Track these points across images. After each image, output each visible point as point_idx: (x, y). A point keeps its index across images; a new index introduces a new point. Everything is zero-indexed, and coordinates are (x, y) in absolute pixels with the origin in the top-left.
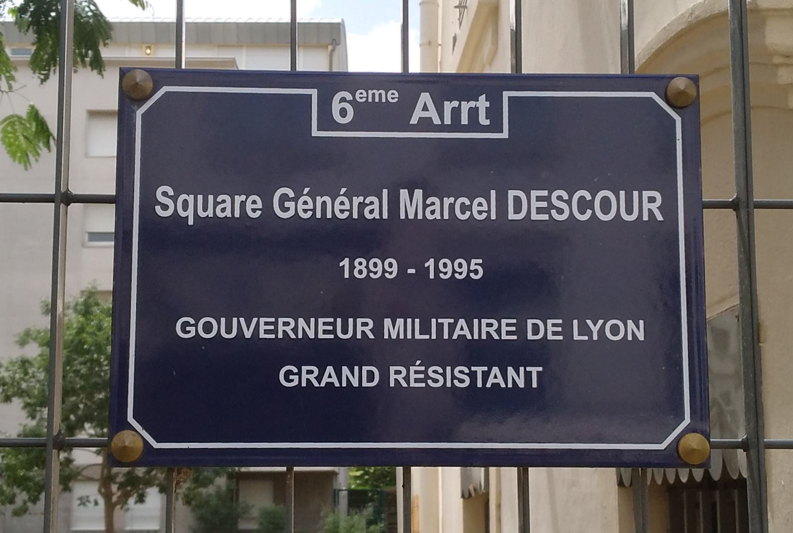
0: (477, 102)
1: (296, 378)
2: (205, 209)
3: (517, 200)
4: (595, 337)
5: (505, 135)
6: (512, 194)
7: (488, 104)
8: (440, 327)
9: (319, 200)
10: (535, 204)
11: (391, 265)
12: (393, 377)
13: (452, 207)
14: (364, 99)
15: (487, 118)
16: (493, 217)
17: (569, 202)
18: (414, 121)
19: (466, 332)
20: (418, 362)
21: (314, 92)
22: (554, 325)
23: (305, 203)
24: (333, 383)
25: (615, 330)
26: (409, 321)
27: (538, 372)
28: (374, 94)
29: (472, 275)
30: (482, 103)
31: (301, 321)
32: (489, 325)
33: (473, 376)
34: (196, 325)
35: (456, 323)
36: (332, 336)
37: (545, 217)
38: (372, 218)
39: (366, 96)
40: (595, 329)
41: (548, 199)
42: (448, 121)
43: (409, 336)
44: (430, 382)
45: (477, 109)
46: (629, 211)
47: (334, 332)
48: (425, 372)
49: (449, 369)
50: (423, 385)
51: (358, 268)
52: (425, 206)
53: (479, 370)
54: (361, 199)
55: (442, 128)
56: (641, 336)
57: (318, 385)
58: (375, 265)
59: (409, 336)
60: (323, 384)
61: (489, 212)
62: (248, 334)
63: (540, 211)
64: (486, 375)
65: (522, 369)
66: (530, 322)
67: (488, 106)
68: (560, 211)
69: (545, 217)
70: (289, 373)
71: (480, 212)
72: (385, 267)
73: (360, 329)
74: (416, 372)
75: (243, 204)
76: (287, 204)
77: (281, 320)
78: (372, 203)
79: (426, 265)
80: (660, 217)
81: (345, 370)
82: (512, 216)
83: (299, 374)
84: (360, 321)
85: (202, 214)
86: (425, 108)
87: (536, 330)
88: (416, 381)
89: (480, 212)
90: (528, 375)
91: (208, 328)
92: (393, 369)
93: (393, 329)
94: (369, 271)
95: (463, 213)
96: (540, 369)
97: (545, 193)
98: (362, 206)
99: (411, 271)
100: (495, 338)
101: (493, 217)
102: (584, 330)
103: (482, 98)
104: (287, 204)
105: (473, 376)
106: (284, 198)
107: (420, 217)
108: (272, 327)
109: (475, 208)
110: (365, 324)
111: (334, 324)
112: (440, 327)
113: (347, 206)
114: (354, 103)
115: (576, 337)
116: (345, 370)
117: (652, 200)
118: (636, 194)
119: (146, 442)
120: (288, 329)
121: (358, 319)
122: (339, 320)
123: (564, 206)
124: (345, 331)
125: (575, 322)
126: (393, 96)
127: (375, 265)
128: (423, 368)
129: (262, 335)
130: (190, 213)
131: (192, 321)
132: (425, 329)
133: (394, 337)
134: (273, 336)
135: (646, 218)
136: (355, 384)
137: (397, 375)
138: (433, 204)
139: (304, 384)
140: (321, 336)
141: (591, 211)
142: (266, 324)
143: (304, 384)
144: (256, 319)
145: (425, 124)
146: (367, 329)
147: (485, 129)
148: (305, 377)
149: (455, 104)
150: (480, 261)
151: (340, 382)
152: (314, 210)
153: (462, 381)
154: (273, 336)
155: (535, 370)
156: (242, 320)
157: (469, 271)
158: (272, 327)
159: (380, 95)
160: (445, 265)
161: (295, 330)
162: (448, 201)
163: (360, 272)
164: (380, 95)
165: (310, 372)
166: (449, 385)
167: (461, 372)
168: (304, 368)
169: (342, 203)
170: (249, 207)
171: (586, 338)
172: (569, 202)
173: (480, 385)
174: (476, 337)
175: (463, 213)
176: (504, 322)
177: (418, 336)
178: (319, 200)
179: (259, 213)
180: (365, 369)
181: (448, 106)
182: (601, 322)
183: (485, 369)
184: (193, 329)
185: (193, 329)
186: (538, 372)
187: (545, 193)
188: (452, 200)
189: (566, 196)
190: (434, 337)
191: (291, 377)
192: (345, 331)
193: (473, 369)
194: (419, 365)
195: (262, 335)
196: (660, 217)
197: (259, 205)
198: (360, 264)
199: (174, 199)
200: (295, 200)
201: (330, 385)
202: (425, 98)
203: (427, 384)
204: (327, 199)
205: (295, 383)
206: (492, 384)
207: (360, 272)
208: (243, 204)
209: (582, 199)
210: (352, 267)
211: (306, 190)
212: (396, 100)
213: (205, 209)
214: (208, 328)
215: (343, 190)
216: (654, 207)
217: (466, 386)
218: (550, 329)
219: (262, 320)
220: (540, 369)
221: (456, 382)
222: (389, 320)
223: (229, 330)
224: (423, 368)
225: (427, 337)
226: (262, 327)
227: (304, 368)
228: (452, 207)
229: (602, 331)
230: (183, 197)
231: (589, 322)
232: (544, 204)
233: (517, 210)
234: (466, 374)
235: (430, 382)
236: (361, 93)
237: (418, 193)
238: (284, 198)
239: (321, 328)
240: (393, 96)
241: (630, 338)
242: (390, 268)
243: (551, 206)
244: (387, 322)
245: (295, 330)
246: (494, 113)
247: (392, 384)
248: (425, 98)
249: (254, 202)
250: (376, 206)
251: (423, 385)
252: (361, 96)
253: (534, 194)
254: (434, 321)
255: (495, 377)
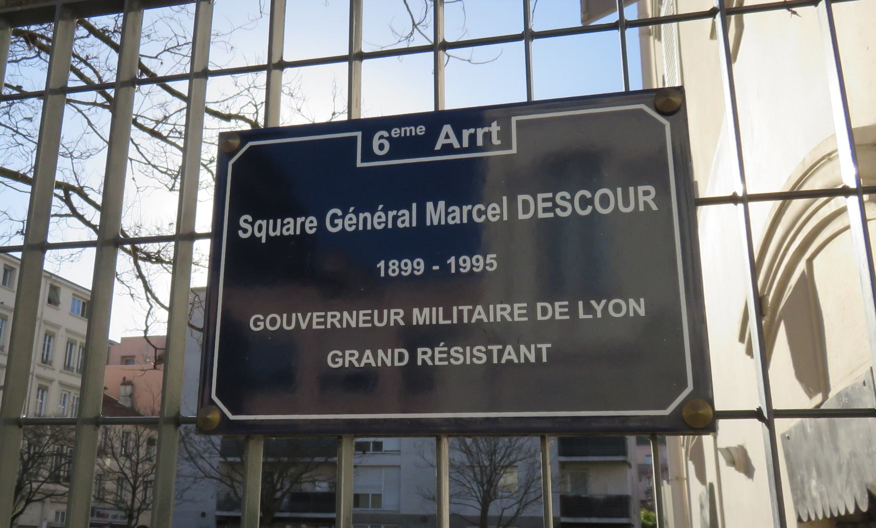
0: (490, 128)
1: (340, 360)
2: (274, 230)
3: (526, 203)
4: (599, 315)
5: (514, 151)
6: (521, 198)
7: (499, 128)
8: (460, 313)
9: (362, 216)
10: (541, 205)
11: (418, 264)
12: (420, 357)
13: (470, 213)
14: (398, 135)
15: (498, 139)
16: (505, 218)
17: (571, 201)
18: (438, 147)
19: (483, 316)
20: (442, 344)
21: (359, 134)
22: (561, 307)
23: (351, 219)
24: (370, 363)
25: (617, 308)
26: (434, 309)
27: (547, 348)
28: (405, 131)
29: (488, 268)
30: (495, 128)
31: (346, 314)
32: (503, 309)
33: (489, 353)
34: (264, 321)
35: (504, 348)
36: (370, 325)
37: (551, 215)
38: (403, 227)
39: (399, 132)
40: (599, 308)
41: (552, 200)
42: (466, 144)
43: (434, 322)
44: (452, 360)
45: (490, 133)
46: (626, 203)
47: (372, 321)
48: (448, 352)
49: (468, 349)
50: (446, 363)
51: (392, 267)
52: (447, 214)
53: (495, 348)
54: (395, 212)
55: (462, 150)
56: (642, 312)
57: (358, 366)
58: (406, 265)
59: (434, 322)
60: (362, 365)
61: (501, 214)
62: (304, 326)
63: (545, 210)
64: (501, 353)
65: (533, 346)
66: (539, 305)
67: (500, 129)
68: (564, 209)
69: (551, 215)
70: (335, 356)
71: (494, 216)
72: (414, 266)
73: (393, 317)
74: (440, 352)
75: (303, 224)
76: (336, 221)
77: (329, 314)
78: (403, 215)
79: (448, 262)
80: (654, 207)
81: (380, 353)
82: (521, 216)
83: (343, 357)
84: (393, 311)
85: (272, 234)
86: (447, 137)
87: (544, 311)
88: (441, 360)
89: (494, 216)
90: (538, 352)
91: (273, 322)
92: (420, 350)
93: (421, 316)
94: (401, 270)
95: (479, 216)
96: (549, 345)
97: (550, 195)
98: (395, 218)
99: (436, 268)
100: (508, 320)
101: (505, 218)
102: (589, 309)
103: (494, 124)
104: (336, 221)
105: (489, 353)
106: (335, 216)
107: (443, 223)
108: (322, 320)
109: (490, 212)
110: (397, 314)
111: (372, 315)
112: (460, 313)
113: (384, 219)
114: (390, 139)
115: (582, 316)
116: (380, 353)
117: (646, 193)
118: (631, 189)
119: (223, 415)
120: (335, 321)
121: (391, 310)
122: (376, 312)
123: (567, 205)
124: (381, 320)
125: (581, 303)
126: (421, 130)
127: (406, 265)
128: (446, 349)
129: (315, 327)
130: (263, 234)
131: (262, 317)
132: (448, 315)
133: (421, 323)
134: (323, 327)
135: (641, 208)
136: (389, 364)
137: (423, 355)
138: (454, 211)
139: (347, 365)
140: (361, 325)
141: (591, 207)
142: (318, 317)
143: (347, 365)
144: (311, 313)
145: (448, 149)
146: (399, 318)
147: (499, 148)
148: (347, 359)
149: (472, 131)
150: (494, 256)
151: (376, 362)
152: (357, 224)
153: (480, 358)
154: (323, 327)
155: (544, 347)
156: (299, 315)
157: (485, 265)
158: (322, 320)
159: (411, 131)
160: (465, 261)
161: (341, 321)
162: (466, 209)
163: (394, 271)
164: (411, 131)
165: (352, 355)
166: (468, 362)
167: (479, 351)
168: (347, 352)
169: (380, 217)
170: (307, 225)
171: (591, 316)
172: (571, 201)
173: (495, 361)
174: (492, 320)
175: (479, 216)
176: (516, 306)
177: (441, 322)
178: (362, 216)
179: (314, 230)
180: (397, 351)
181: (466, 133)
182: (604, 302)
183: (471, 307)
184: (262, 324)
185: (262, 324)
186: (547, 348)
187: (550, 195)
188: (470, 207)
189: (568, 196)
190: (455, 321)
191: (337, 360)
192: (381, 320)
193: (490, 347)
194: (443, 346)
195: (315, 327)
196: (654, 207)
197: (315, 224)
198: (394, 264)
199: (252, 224)
200: (343, 217)
201: (368, 365)
202: (447, 129)
203: (450, 363)
204: (368, 215)
205: (340, 365)
206: (477, 319)
207: (394, 271)
208: (303, 224)
209: (583, 198)
210: (387, 267)
211: (352, 209)
212: (423, 133)
213: (274, 230)
214: (273, 322)
215: (381, 207)
216: (649, 199)
217: (484, 362)
218: (558, 310)
219: (315, 314)
220: (549, 345)
221: (475, 360)
222: (417, 309)
223: (289, 323)
224: (446, 349)
225: (449, 322)
226: (315, 320)
227: (347, 352)
228: (470, 213)
229: (606, 308)
230: (259, 222)
231: (593, 302)
232: (549, 204)
233: (526, 210)
234: (484, 352)
235: (452, 360)
236: (396, 131)
237: (442, 204)
238: (335, 216)
239: (361, 318)
240: (421, 130)
241: (632, 314)
242: (418, 266)
243: (556, 205)
244: (416, 311)
245: (341, 321)
246: (505, 135)
247: (419, 363)
248: (447, 129)
249: (311, 222)
250: (407, 218)
251: (446, 363)
252: (395, 133)
253: (540, 196)
254: (455, 309)
255: (509, 353)
